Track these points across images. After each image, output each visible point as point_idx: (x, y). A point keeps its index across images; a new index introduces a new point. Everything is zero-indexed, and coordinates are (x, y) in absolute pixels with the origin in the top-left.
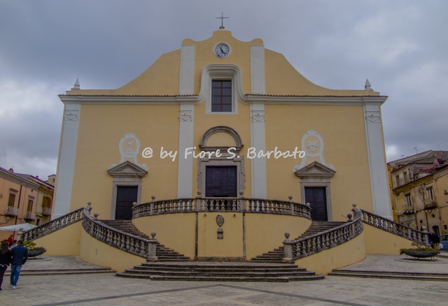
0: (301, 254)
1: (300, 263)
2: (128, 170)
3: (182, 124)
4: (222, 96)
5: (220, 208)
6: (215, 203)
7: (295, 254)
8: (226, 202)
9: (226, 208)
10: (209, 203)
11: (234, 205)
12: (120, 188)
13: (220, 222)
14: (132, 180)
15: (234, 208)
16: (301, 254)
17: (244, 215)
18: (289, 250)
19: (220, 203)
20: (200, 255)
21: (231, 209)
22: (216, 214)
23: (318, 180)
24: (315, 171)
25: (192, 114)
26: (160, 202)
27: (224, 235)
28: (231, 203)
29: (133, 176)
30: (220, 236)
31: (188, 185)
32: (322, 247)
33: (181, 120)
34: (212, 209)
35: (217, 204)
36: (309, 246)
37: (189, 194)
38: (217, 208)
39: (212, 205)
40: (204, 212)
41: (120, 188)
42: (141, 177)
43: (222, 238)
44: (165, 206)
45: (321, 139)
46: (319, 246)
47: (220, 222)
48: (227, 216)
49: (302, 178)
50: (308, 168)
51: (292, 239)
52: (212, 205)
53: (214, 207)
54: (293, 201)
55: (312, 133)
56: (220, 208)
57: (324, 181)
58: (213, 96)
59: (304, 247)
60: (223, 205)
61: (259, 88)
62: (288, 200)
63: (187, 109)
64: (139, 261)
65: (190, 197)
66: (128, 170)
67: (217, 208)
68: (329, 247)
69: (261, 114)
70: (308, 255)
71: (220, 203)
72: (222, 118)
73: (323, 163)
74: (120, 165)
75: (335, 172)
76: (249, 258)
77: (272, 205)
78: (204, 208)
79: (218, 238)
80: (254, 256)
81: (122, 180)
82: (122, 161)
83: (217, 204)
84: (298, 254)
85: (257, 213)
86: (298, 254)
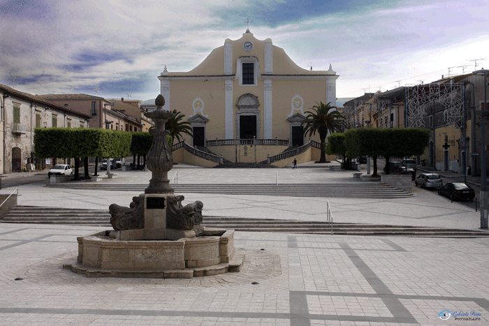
1: (272, 164)
2: (198, 119)
3: (226, 92)
4: (248, 74)
13: (246, 149)
14: (200, 124)
18: (269, 160)
20: (238, 161)
24: (298, 118)
25: (232, 86)
31: (230, 128)
42: (205, 123)
44: (222, 142)
45: (302, 99)
47: (246, 149)
48: (248, 146)
49: (291, 122)
50: (294, 116)
51: (270, 156)
55: (297, 96)
61: (269, 69)
62: (275, 139)
63: (229, 82)
64: (218, 164)
65: (232, 138)
66: (198, 119)
72: (248, 88)
82: (195, 114)
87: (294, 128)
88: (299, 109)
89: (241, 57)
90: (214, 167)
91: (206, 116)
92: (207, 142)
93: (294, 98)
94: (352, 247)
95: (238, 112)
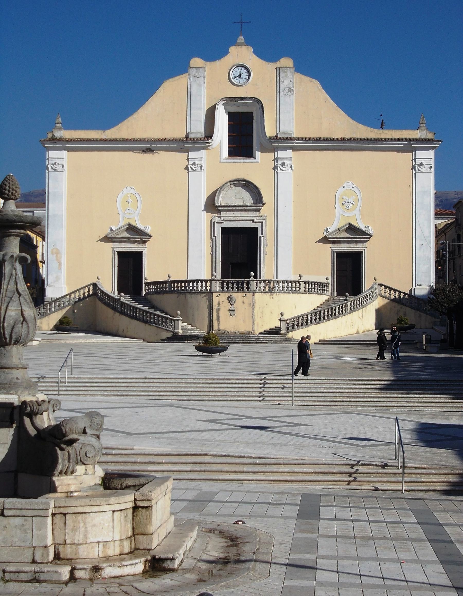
0: (293, 327)
1: (290, 335)
5: (233, 288)
6: (228, 284)
7: (288, 328)
8: (238, 282)
9: (238, 288)
10: (223, 284)
11: (245, 285)
12: (122, 255)
14: (135, 245)
15: (245, 289)
16: (293, 327)
17: (254, 295)
19: (233, 284)
20: (215, 327)
21: (243, 290)
22: (227, 295)
23: (352, 245)
26: (174, 282)
27: (236, 312)
28: (243, 284)
29: (135, 242)
30: (232, 313)
32: (311, 323)
33: (190, 170)
34: (225, 289)
35: (230, 285)
36: (300, 322)
37: (205, 275)
38: (230, 289)
39: (225, 285)
40: (218, 292)
41: (119, 253)
42: (144, 242)
43: (234, 315)
46: (309, 322)
51: (286, 317)
52: (225, 285)
53: (228, 288)
54: (302, 279)
56: (233, 288)
57: (360, 245)
58: (229, 147)
59: (296, 323)
60: (235, 285)
62: (297, 278)
67: (230, 289)
68: (318, 323)
69: (287, 162)
70: (299, 329)
71: (233, 284)
73: (362, 227)
74: (119, 228)
75: (371, 236)
76: (257, 333)
77: (281, 284)
78: (218, 288)
79: (231, 315)
80: (262, 331)
81: (123, 245)
83: (230, 285)
84: (291, 328)
85: (266, 293)
86: (291, 328)
87: (341, 256)
88: (353, 214)
89: (224, 99)
90: (163, 341)
91: (149, 231)
92: (147, 284)
93: (341, 190)
94: (441, 518)
95: (218, 219)
